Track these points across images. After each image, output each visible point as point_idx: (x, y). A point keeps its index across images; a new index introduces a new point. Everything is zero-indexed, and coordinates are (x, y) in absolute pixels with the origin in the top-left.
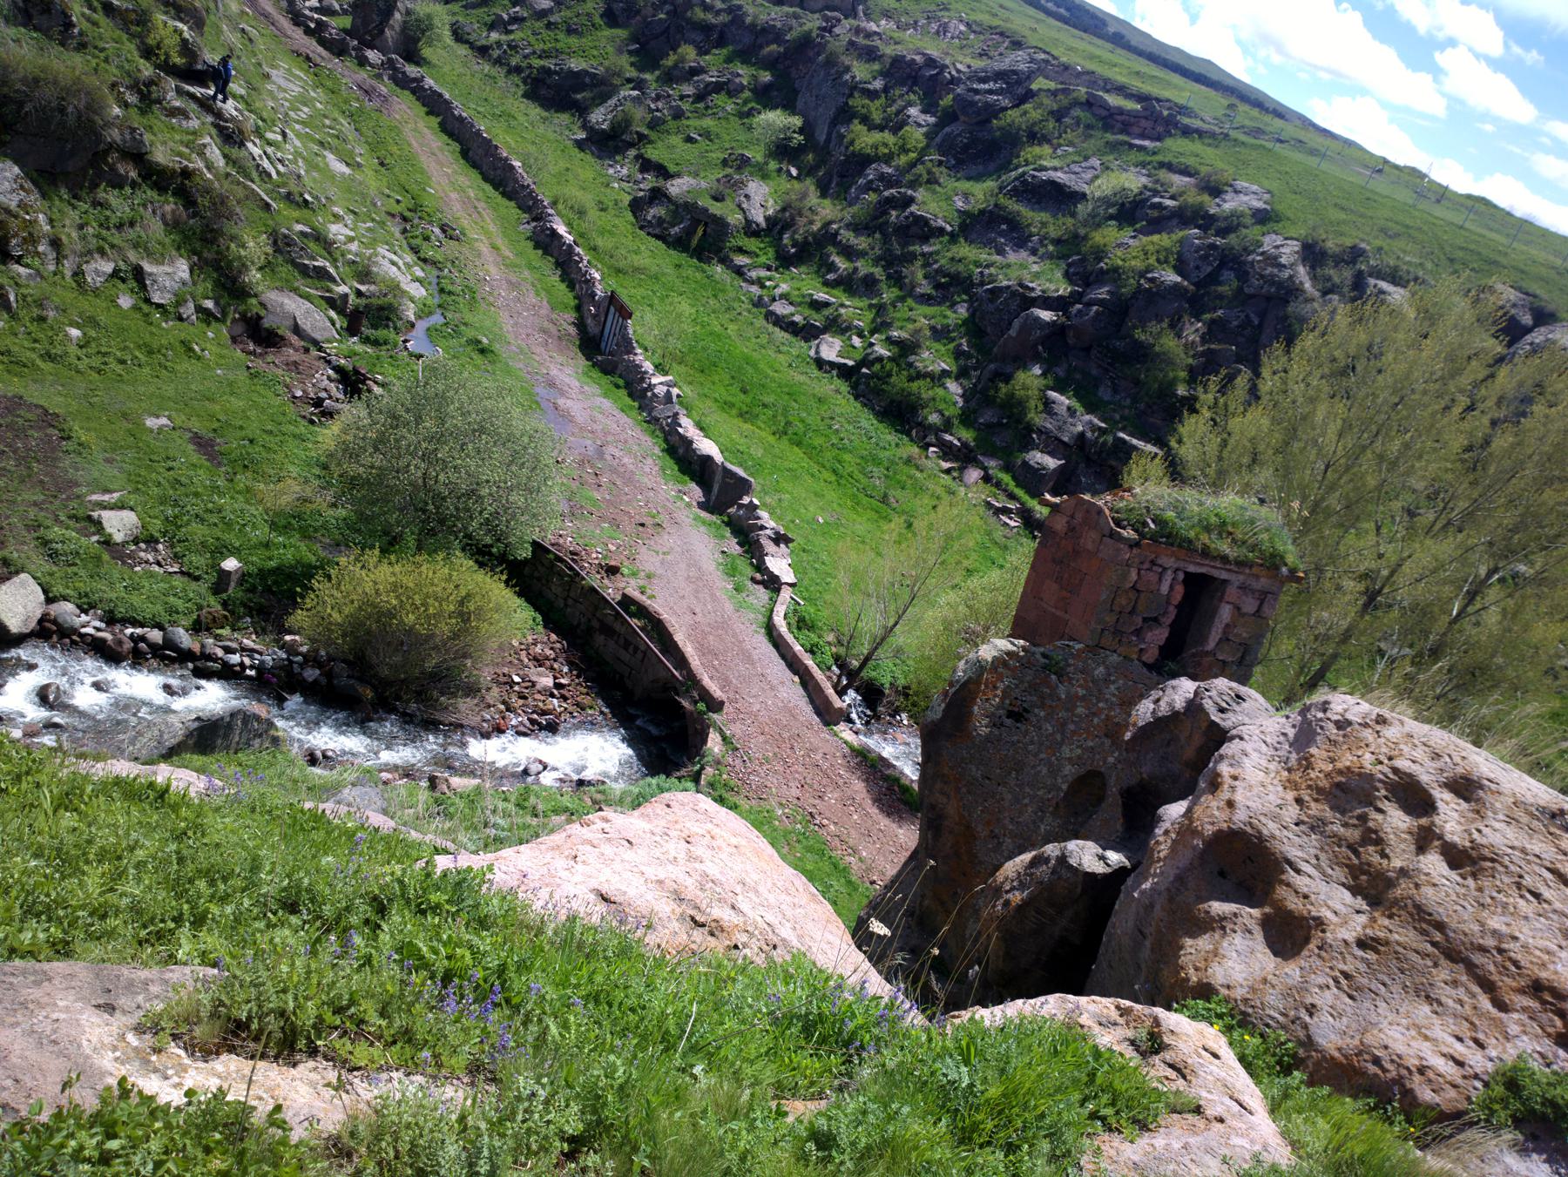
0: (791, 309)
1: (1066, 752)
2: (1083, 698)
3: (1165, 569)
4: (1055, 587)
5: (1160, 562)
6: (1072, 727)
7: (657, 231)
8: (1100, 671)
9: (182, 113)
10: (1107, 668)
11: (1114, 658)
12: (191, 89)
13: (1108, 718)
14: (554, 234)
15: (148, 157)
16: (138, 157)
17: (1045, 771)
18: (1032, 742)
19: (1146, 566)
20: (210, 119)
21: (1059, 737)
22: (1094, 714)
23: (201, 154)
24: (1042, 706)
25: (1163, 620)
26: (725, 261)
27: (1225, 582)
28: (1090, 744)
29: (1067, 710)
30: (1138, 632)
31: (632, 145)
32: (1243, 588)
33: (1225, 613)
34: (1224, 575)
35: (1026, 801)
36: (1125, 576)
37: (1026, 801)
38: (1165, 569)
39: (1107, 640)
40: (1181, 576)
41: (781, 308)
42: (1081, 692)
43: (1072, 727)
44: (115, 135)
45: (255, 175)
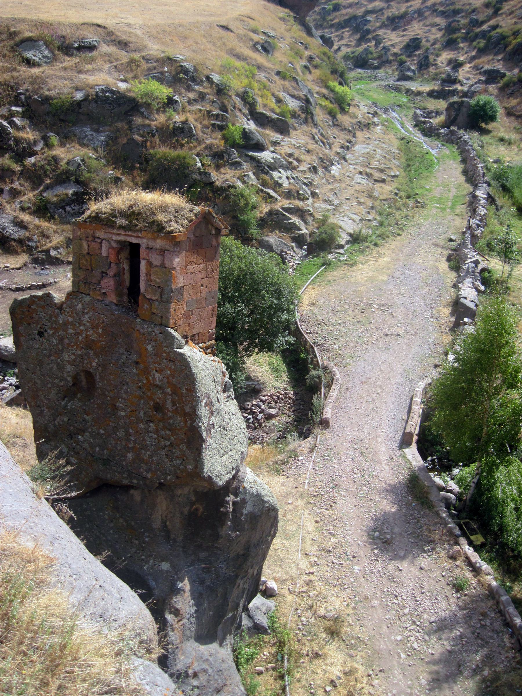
1: (65, 356)
2: (72, 323)
8: (79, 306)
9: (239, 164)
10: (82, 304)
11: (87, 299)
17: (55, 367)
24: (52, 328)
28: (80, 353)
29: (64, 331)
35: (49, 386)
36: (81, 246)
37: (49, 386)
39: (82, 288)
42: (71, 319)
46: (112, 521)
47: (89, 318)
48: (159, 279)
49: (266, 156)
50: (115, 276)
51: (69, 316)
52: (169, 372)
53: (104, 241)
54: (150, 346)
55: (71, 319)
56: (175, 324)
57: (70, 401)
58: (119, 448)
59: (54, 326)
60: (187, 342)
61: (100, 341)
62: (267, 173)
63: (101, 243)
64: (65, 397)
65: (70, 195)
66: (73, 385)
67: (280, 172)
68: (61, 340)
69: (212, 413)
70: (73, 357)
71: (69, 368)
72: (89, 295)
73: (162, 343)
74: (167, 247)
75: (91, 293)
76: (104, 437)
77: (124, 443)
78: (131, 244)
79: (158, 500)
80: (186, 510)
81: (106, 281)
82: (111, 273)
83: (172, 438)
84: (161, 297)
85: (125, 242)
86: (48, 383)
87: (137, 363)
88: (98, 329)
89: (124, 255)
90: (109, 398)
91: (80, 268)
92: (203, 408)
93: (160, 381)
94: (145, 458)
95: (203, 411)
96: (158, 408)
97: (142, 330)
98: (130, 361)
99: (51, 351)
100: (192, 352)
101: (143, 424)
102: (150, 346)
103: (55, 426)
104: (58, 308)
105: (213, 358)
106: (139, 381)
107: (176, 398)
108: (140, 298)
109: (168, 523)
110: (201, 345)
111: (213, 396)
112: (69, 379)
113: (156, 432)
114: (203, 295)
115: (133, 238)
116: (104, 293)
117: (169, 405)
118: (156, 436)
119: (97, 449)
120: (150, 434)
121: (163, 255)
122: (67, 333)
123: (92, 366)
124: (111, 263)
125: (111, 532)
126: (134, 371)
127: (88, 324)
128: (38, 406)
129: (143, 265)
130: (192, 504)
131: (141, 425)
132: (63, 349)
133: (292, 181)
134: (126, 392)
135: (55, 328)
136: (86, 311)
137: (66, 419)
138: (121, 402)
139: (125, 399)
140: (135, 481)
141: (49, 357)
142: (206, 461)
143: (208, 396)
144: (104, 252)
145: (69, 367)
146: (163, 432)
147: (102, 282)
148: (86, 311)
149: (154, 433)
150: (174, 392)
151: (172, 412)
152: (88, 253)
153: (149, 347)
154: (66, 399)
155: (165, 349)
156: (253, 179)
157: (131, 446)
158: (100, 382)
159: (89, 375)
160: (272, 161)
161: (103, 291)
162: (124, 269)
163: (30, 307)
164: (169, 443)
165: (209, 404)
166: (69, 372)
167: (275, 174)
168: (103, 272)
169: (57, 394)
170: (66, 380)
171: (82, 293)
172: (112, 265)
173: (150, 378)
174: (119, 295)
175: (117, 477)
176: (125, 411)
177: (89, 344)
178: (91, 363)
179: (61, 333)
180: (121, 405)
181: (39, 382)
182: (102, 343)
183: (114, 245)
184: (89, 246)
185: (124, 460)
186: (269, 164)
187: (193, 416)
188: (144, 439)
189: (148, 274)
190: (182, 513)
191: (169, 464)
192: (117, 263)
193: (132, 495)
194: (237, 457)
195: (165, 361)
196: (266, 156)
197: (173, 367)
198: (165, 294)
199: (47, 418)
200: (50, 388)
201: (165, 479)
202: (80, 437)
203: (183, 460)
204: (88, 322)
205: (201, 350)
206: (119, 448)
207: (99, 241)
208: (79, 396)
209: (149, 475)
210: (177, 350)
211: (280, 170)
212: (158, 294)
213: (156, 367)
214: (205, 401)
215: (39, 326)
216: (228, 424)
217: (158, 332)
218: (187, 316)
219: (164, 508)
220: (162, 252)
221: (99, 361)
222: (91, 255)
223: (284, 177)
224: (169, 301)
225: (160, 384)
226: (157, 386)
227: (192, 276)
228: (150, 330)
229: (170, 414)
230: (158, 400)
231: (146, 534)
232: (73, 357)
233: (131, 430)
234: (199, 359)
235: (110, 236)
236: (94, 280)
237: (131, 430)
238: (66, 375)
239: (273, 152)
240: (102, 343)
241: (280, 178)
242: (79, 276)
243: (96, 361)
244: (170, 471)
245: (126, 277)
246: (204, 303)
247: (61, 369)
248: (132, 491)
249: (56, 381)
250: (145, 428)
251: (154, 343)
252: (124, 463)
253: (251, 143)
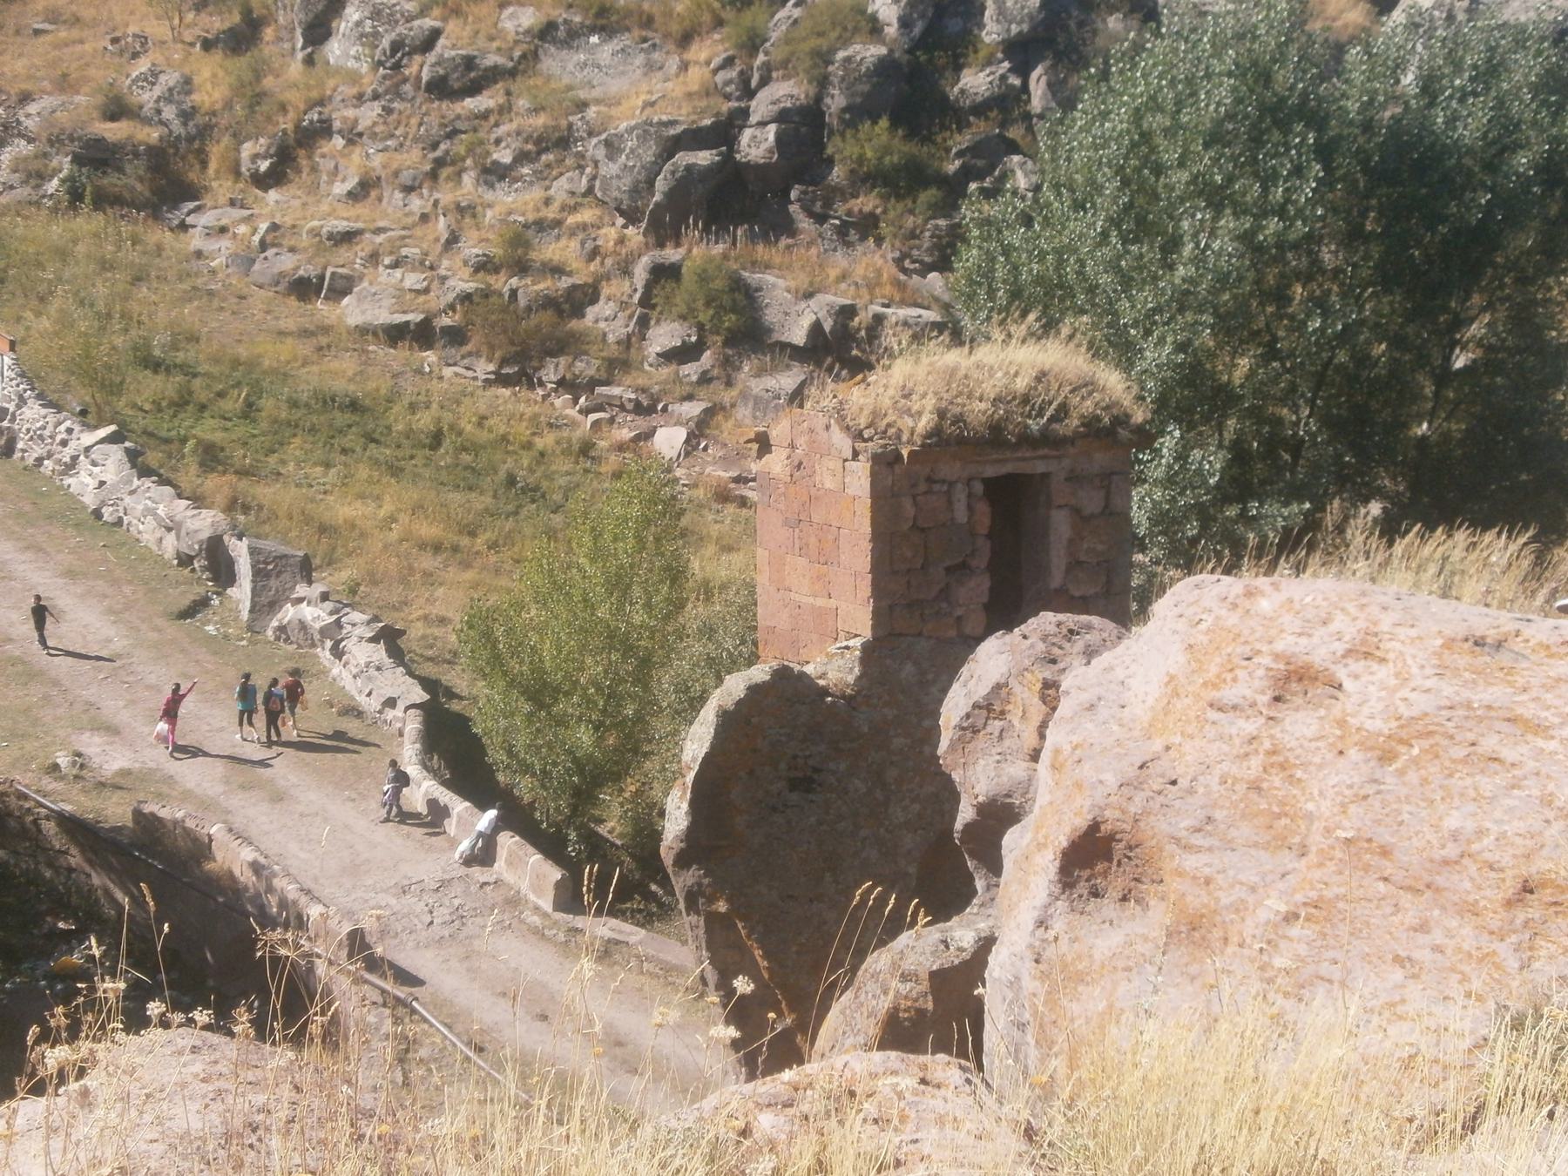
3: (951, 484)
4: (802, 561)
19: (922, 487)
21: (879, 794)
25: (974, 563)
27: (1045, 476)
30: (945, 593)
32: (1074, 478)
33: (1061, 525)
34: (1040, 467)
38: (951, 484)
40: (979, 488)
42: (890, 713)
53: (960, 486)
55: (890, 713)
70: (917, 807)
72: (920, 634)
148: (930, 677)
207: (945, 488)
215: (783, 766)
222: (923, 530)
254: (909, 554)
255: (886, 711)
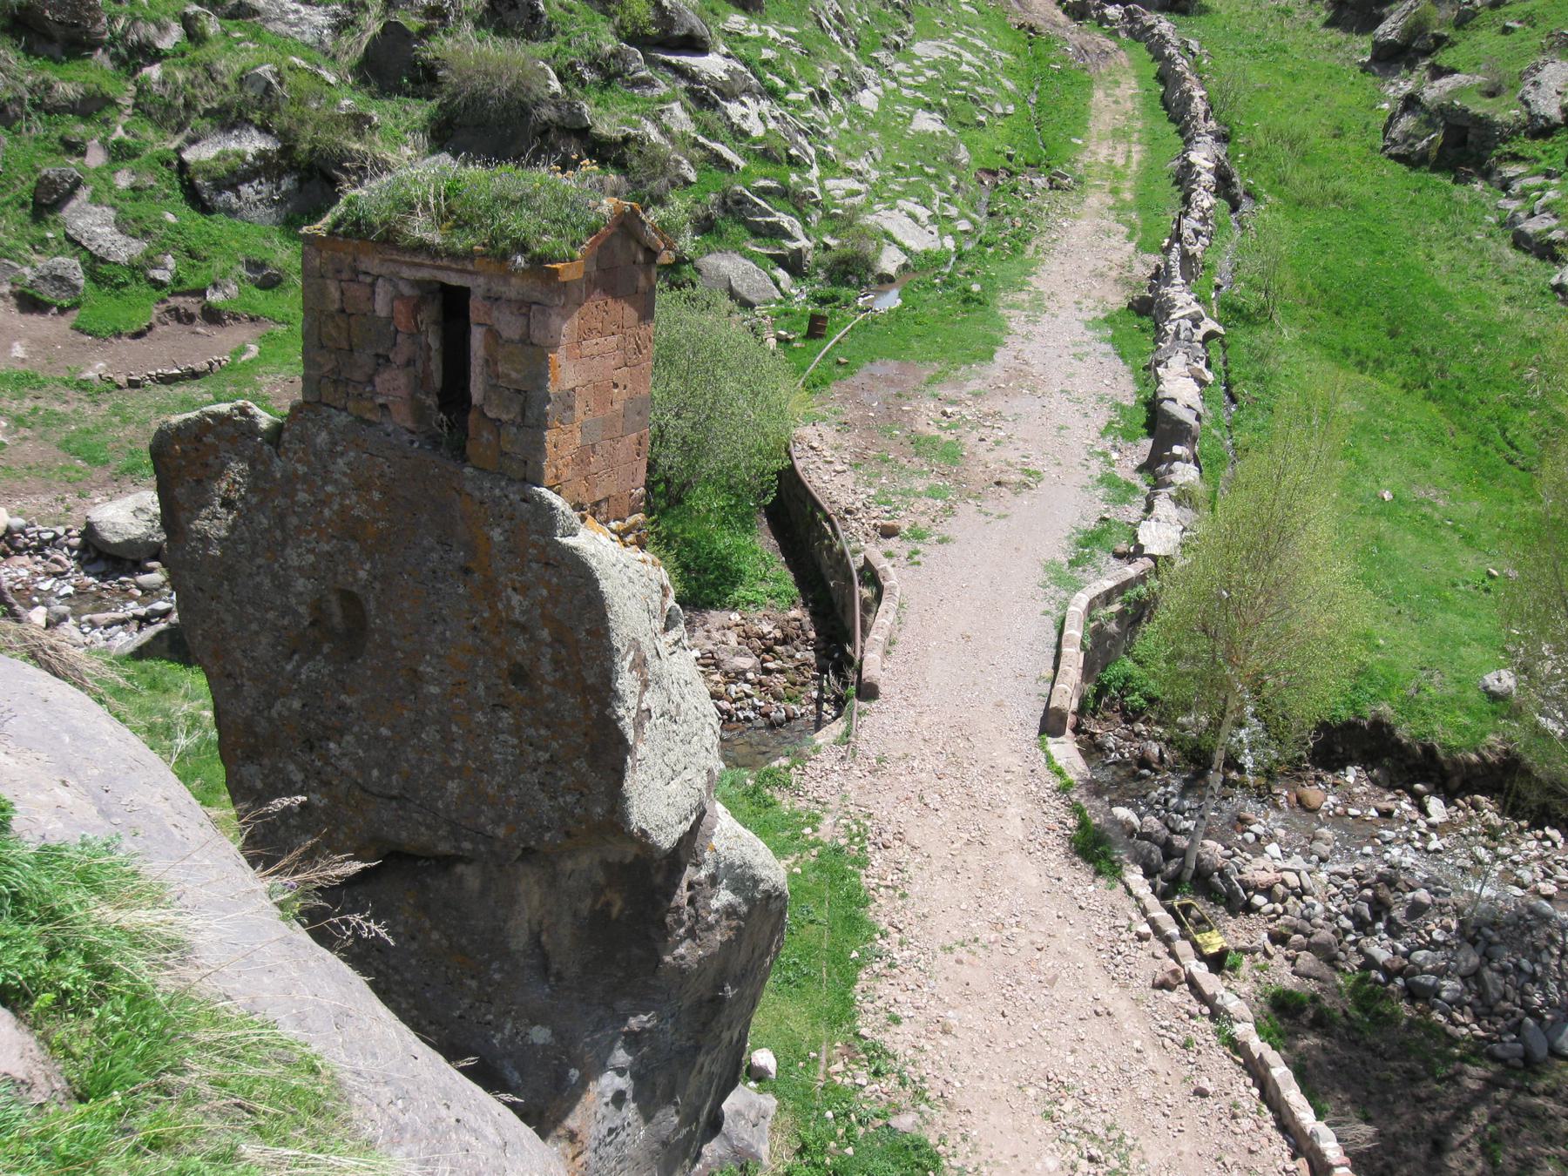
0: (1555, 222)
1: (292, 556)
2: (305, 478)
5: (363, 267)
6: (294, 521)
7: (1402, 150)
8: (323, 438)
9: (648, 83)
10: (330, 433)
11: (342, 419)
12: (668, 58)
13: (344, 510)
14: (1190, 165)
15: (593, 131)
16: (582, 133)
18: (243, 541)
19: (345, 276)
20: (684, 84)
21: (278, 534)
22: (324, 503)
23: (656, 120)
26: (1486, 175)
28: (327, 548)
29: (285, 496)
31: (1427, 53)
35: (254, 627)
36: (322, 293)
37: (254, 627)
41: (1531, 227)
43: (294, 521)
44: (547, 113)
45: (724, 133)
46: (413, 938)
47: (348, 464)
48: (518, 371)
49: (712, 65)
50: (410, 362)
51: (299, 461)
52: (545, 592)
53: (380, 281)
54: (499, 530)
55: (301, 469)
56: (557, 477)
57: (303, 661)
58: (427, 770)
59: (261, 484)
60: (583, 519)
61: (377, 520)
62: (715, 106)
63: (373, 285)
64: (294, 652)
65: (249, 158)
66: (312, 624)
67: (743, 104)
68: (281, 519)
69: (645, 685)
70: (311, 558)
71: (301, 584)
72: (345, 409)
73: (527, 523)
74: (537, 296)
75: (351, 405)
76: (391, 744)
77: (438, 758)
78: (445, 289)
79: (522, 887)
80: (585, 906)
81: (386, 376)
82: (399, 358)
83: (555, 745)
84: (523, 415)
85: (430, 282)
86: (250, 622)
87: (467, 571)
88: (369, 490)
89: (429, 314)
90: (400, 655)
91: (322, 347)
92: (627, 674)
93: (523, 613)
94: (489, 790)
95: (626, 682)
96: (519, 675)
97: (477, 493)
98: (450, 567)
99: (256, 543)
100: (594, 543)
101: (485, 714)
102: (499, 530)
103: (270, 720)
104: (270, 442)
105: (641, 556)
106: (474, 612)
107: (563, 652)
108: (472, 417)
109: (544, 938)
110: (613, 525)
111: (646, 643)
112: (302, 609)
113: (516, 730)
114: (616, 406)
115: (452, 274)
116: (381, 406)
117: (546, 667)
118: (516, 741)
119: (375, 773)
120: (502, 737)
121: (527, 316)
122: (294, 503)
123: (356, 580)
124: (397, 331)
125: (413, 962)
126: (461, 591)
127: (346, 480)
128: (229, 676)
129: (477, 338)
130: (597, 891)
131: (480, 717)
132: (285, 539)
133: (772, 125)
134: (443, 640)
135: (264, 490)
136: (339, 449)
137: (296, 704)
138: (429, 664)
139: (439, 656)
140: (467, 845)
141: (251, 559)
142: (635, 795)
143: (636, 645)
144: (381, 307)
145: (301, 581)
146: (532, 731)
147: (377, 380)
148: (339, 449)
149: (510, 734)
150: (558, 640)
151: (553, 684)
152: (343, 311)
153: (497, 535)
154: (296, 657)
155: (535, 537)
156: (680, 117)
157: (454, 764)
158: (377, 616)
159: (350, 599)
160: (726, 77)
161: (381, 400)
162: (430, 348)
163: (200, 440)
164: (547, 756)
165: (640, 664)
166: (301, 594)
167: (734, 109)
168: (378, 356)
169: (274, 647)
170: (295, 612)
171: (328, 405)
172: (400, 339)
173: (500, 606)
174: (419, 413)
175: (424, 836)
176: (440, 684)
177: (350, 528)
178: (355, 572)
179: (279, 501)
180: (429, 669)
181: (229, 618)
182: (381, 524)
183: (406, 290)
184: (342, 293)
185: (441, 797)
186: (719, 85)
187: (605, 693)
188: (486, 749)
189: (490, 362)
190: (575, 915)
191: (547, 804)
192: (411, 335)
193: (461, 879)
194: (701, 782)
195: (534, 565)
196: (712, 65)
197: (555, 580)
198: (530, 406)
199: (250, 702)
200: (257, 633)
201: (540, 839)
202: (332, 745)
203: (582, 794)
204: (345, 474)
205: (615, 537)
206: (427, 770)
207: (369, 280)
208: (326, 648)
209: (501, 832)
210: (565, 541)
211: (744, 99)
212: (516, 409)
213: (513, 581)
214: (630, 658)
216: (678, 706)
217: (518, 497)
218: (582, 458)
219: (535, 902)
220: (525, 307)
221: (374, 567)
223: (754, 117)
224: (542, 424)
225: (523, 619)
226: (517, 624)
227: (595, 362)
228: (497, 492)
229: (547, 690)
230: (519, 658)
231: (495, 965)
232: (311, 558)
233: (454, 728)
234: (613, 560)
235: (393, 268)
236: (358, 375)
237: (454, 728)
238: (293, 601)
239: (728, 56)
240: (381, 524)
241: (745, 117)
242: (321, 366)
243: (368, 566)
244: (550, 820)
245: (433, 367)
246: (619, 425)
247: (283, 586)
248: (460, 868)
249: (271, 615)
250: (490, 724)
251: (506, 524)
252: (440, 804)
253: (676, 33)
254: (334, 333)
255: (298, 466)
